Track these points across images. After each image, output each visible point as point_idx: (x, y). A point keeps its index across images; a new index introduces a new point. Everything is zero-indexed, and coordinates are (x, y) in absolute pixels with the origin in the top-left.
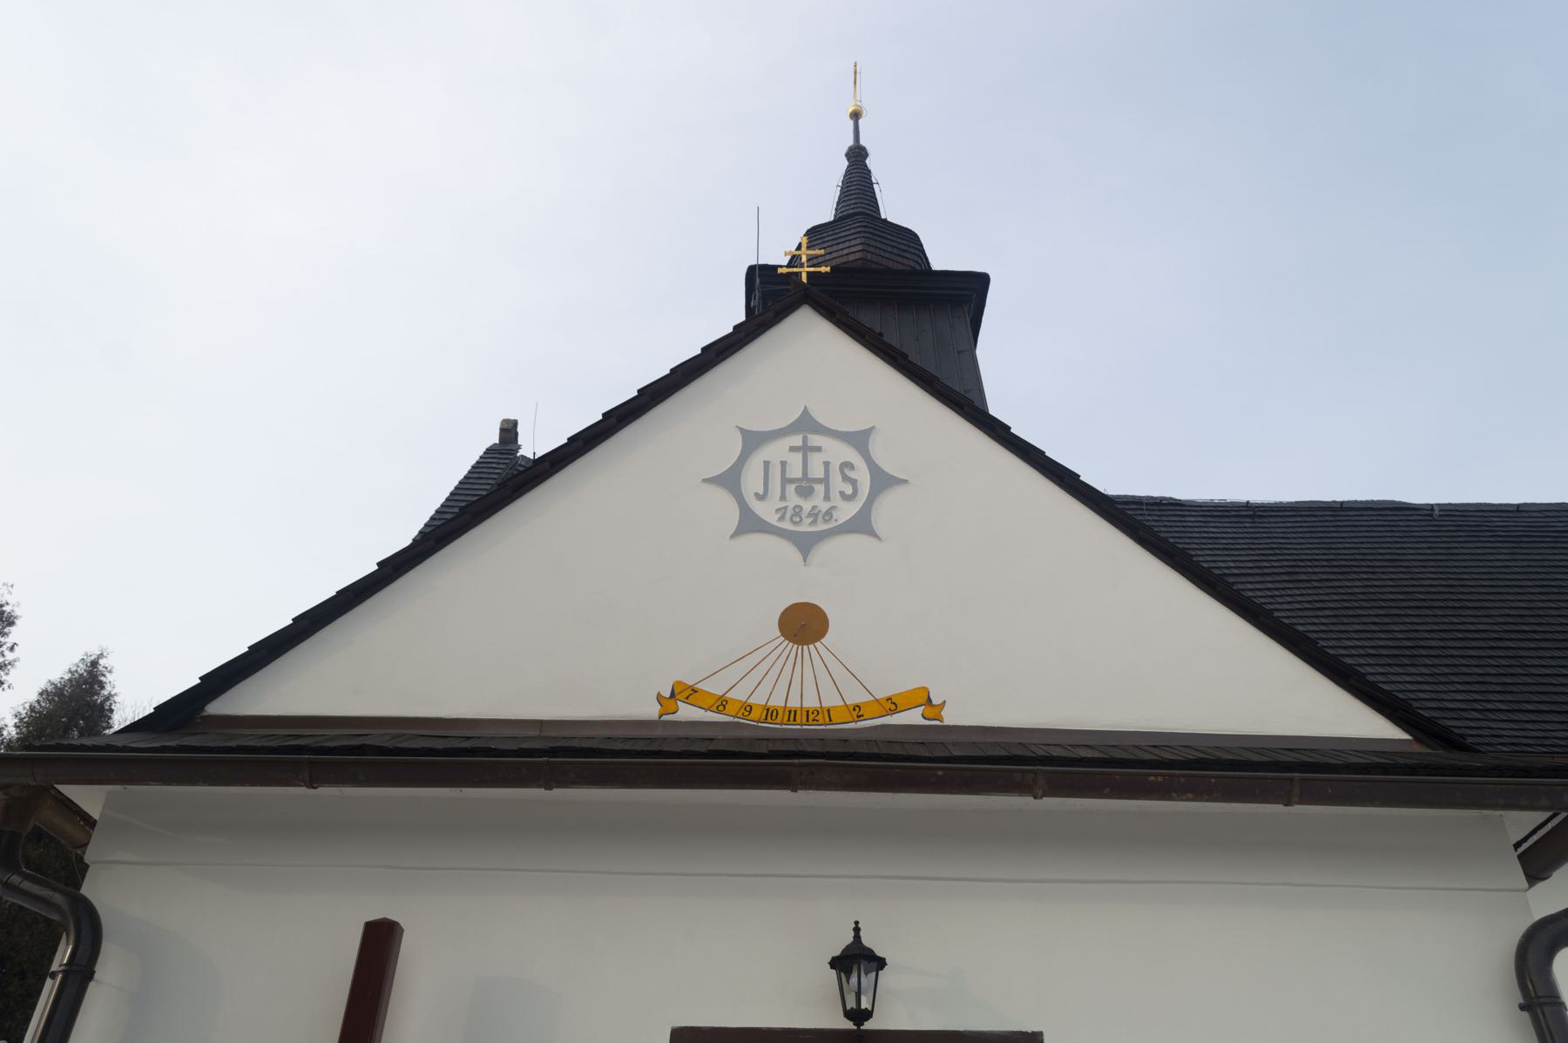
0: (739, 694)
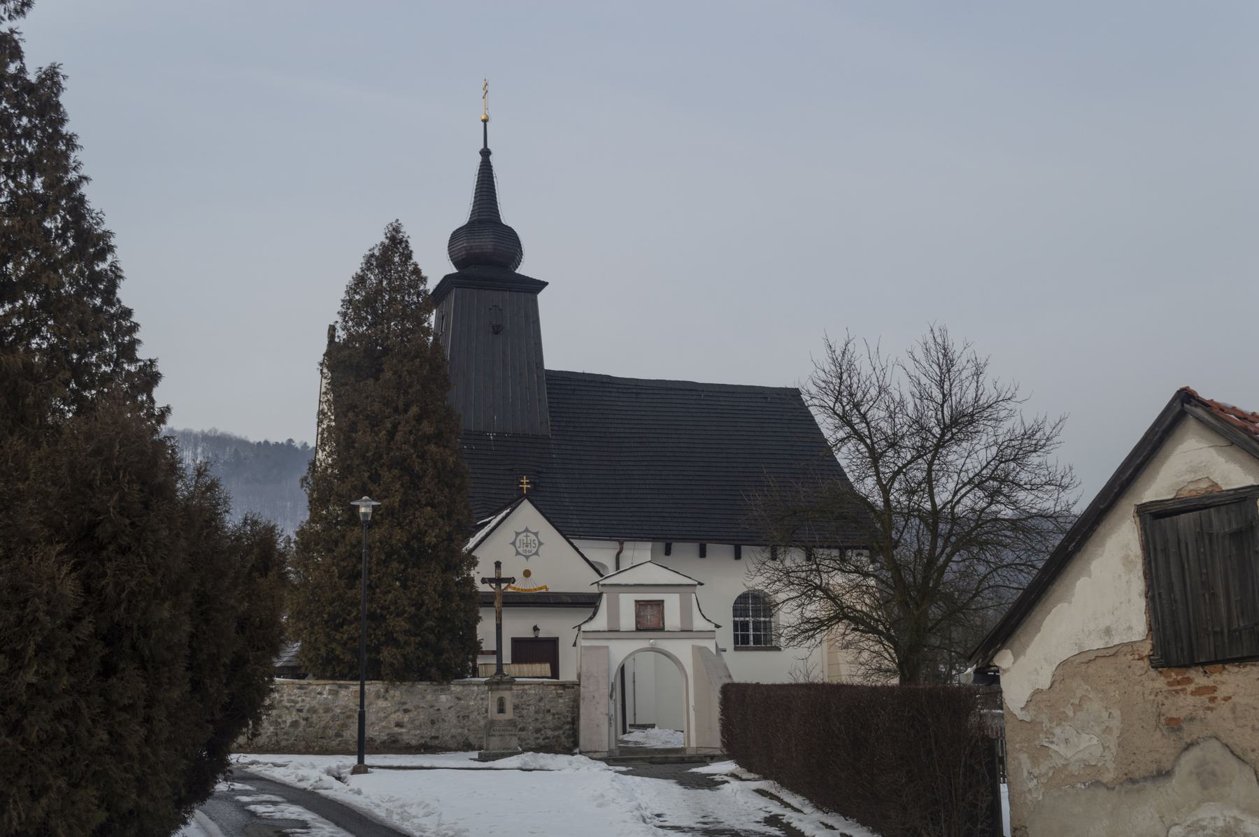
0: (517, 587)
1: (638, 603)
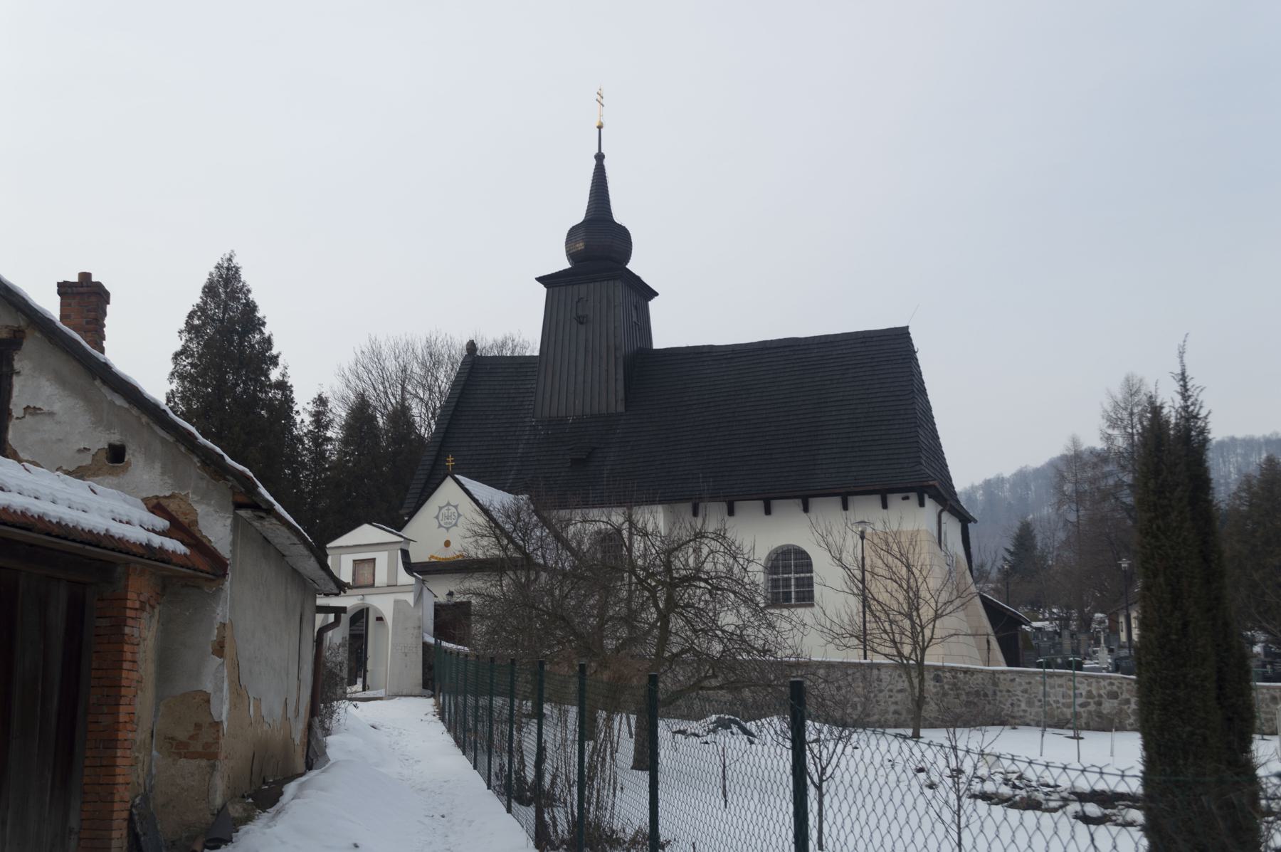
1: (356, 563)
